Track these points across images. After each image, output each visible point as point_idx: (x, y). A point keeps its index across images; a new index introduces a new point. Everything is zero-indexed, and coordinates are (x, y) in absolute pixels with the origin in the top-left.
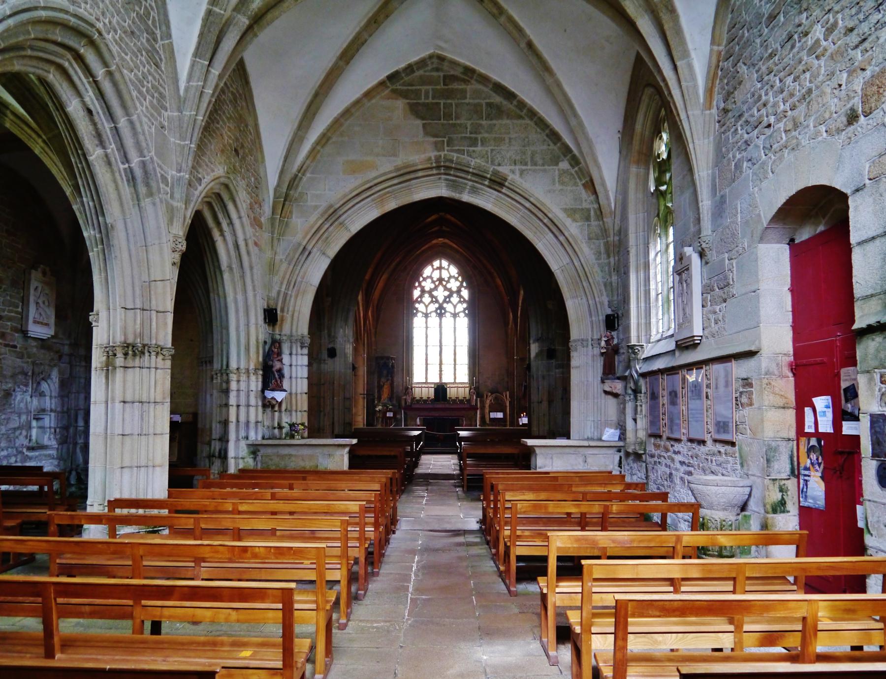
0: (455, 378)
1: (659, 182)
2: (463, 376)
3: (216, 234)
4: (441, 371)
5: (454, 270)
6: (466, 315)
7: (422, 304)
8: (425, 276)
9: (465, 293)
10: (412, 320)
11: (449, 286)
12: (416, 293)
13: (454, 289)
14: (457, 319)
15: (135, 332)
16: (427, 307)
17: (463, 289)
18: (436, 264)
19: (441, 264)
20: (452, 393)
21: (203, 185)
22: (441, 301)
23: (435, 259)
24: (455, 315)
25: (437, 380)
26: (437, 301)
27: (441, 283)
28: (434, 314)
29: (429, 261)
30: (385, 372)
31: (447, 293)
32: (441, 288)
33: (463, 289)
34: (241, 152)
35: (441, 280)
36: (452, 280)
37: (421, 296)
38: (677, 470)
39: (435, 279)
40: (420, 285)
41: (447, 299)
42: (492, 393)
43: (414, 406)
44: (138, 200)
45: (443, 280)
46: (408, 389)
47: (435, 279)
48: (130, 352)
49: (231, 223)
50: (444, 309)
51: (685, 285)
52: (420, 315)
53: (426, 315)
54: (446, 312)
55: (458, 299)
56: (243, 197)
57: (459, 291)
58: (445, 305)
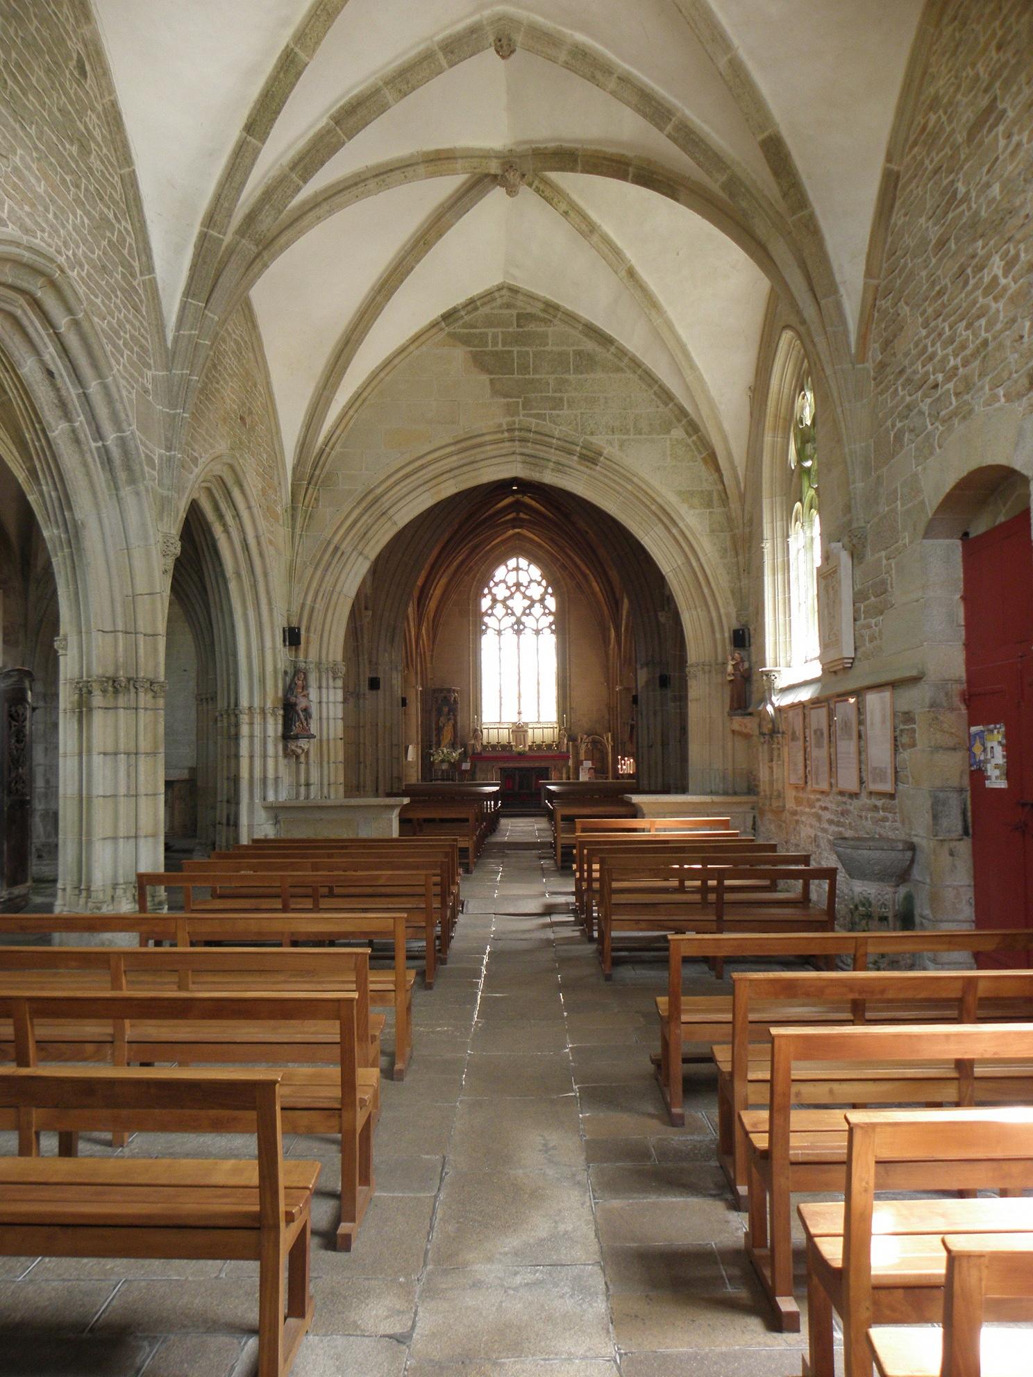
1: (801, 456)
2: (550, 713)
3: (218, 530)
5: (535, 572)
8: (496, 579)
9: (551, 603)
11: (528, 593)
12: (486, 603)
15: (116, 661)
17: (548, 597)
18: (512, 563)
21: (200, 467)
22: (518, 614)
23: (511, 557)
24: (537, 632)
25: (515, 720)
26: (513, 614)
27: (518, 589)
29: (502, 560)
30: (446, 709)
31: (527, 603)
32: (518, 596)
33: (548, 597)
34: (248, 420)
35: (518, 585)
36: (534, 585)
37: (492, 607)
38: (824, 830)
39: (510, 584)
40: (490, 592)
41: (527, 611)
43: (484, 754)
44: (117, 489)
46: (477, 733)
47: (510, 584)
48: (111, 689)
49: (237, 516)
50: (523, 624)
51: (831, 592)
53: (499, 633)
56: (253, 483)
57: (542, 600)
58: (524, 619)
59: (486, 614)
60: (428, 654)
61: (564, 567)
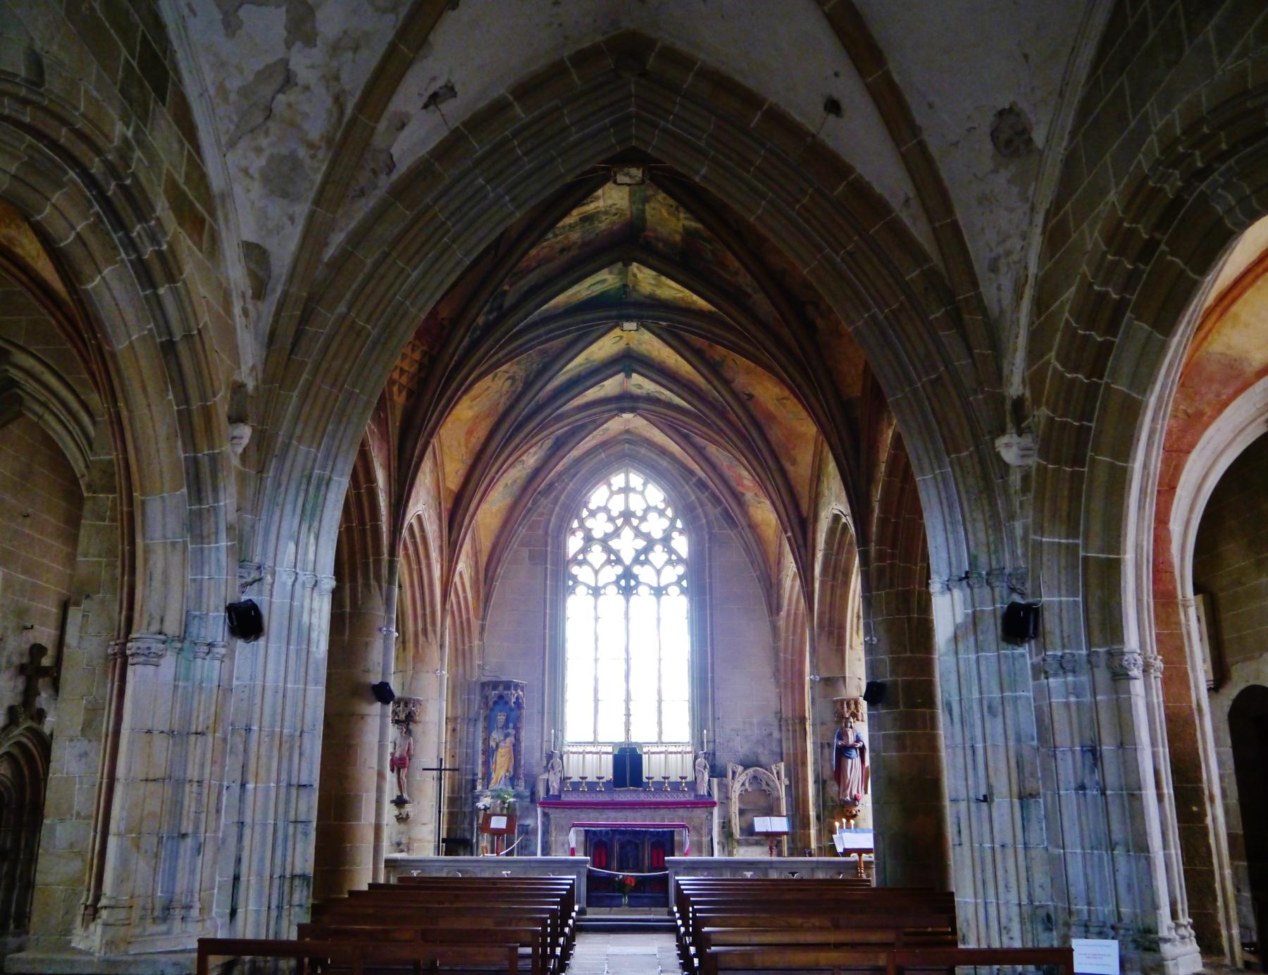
0: (660, 733)
2: (679, 728)
4: (628, 715)
5: (656, 495)
6: (683, 591)
7: (585, 567)
8: (592, 506)
9: (681, 544)
10: (564, 600)
11: (644, 528)
12: (574, 544)
13: (657, 534)
14: (664, 598)
16: (596, 572)
17: (675, 534)
18: (618, 480)
19: (627, 481)
20: (653, 767)
23: (616, 471)
24: (659, 591)
25: (620, 738)
26: (619, 561)
27: (627, 521)
28: (613, 589)
29: (599, 474)
31: (641, 544)
32: (627, 533)
33: (675, 534)
35: (627, 515)
36: (652, 516)
37: (584, 550)
39: (615, 513)
40: (582, 526)
41: (641, 558)
42: (746, 767)
43: (564, 798)
45: (633, 514)
46: (551, 759)
47: (615, 513)
50: (635, 577)
52: (581, 590)
53: (596, 591)
54: (638, 583)
55: (666, 556)
57: (666, 540)
58: (637, 569)
59: (575, 560)
60: (476, 624)
61: (701, 485)
